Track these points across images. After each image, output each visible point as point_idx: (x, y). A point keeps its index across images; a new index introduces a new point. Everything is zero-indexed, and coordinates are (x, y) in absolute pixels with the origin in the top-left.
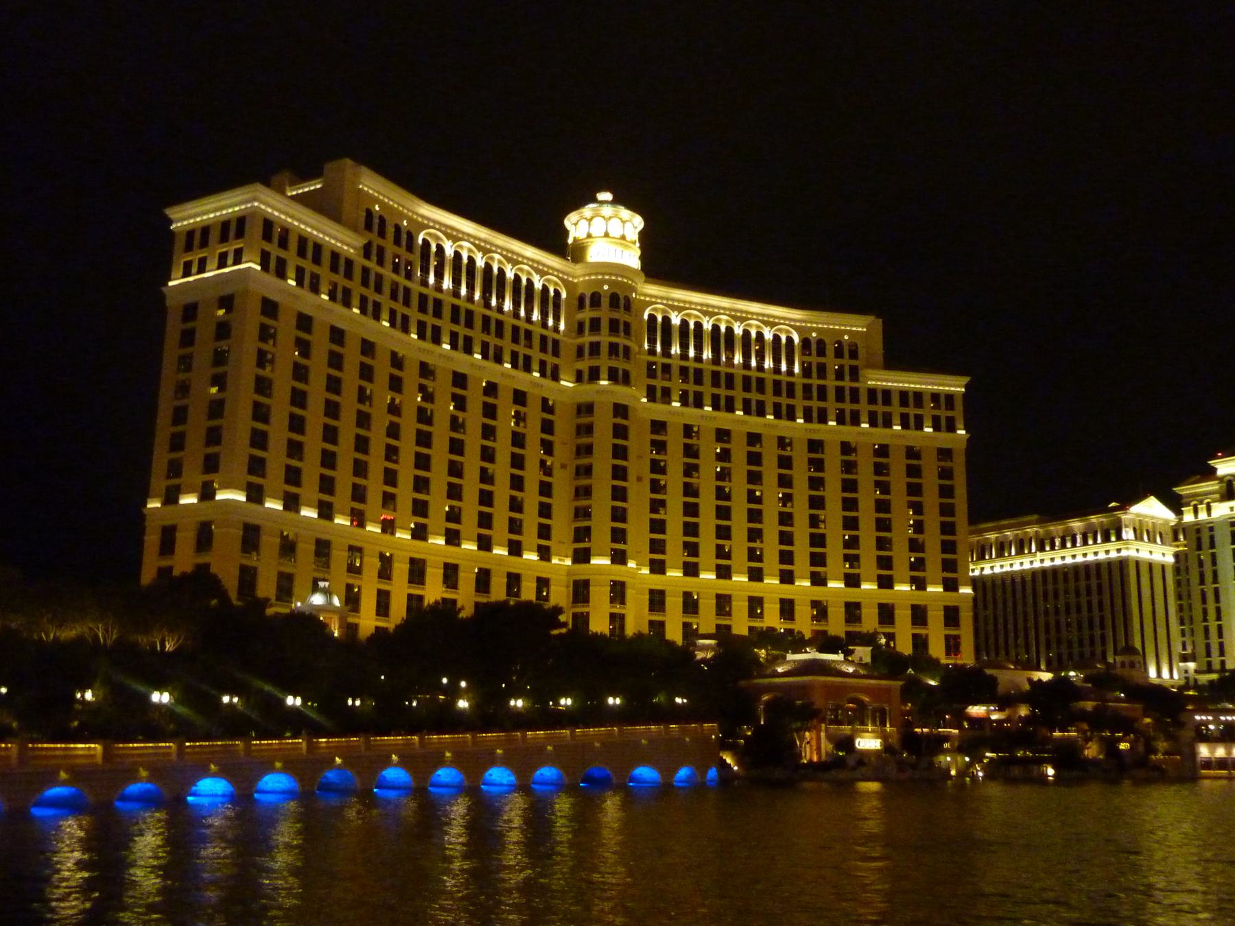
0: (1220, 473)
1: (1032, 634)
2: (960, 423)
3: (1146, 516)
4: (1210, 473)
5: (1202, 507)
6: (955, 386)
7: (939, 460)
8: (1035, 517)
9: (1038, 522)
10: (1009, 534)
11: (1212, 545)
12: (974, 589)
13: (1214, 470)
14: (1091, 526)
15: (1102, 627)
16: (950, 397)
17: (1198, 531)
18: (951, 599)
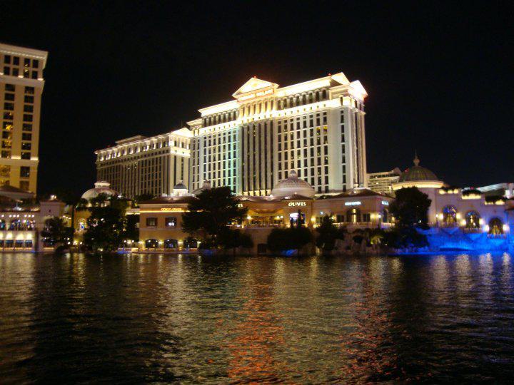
0: (203, 115)
1: (137, 188)
2: (40, 74)
3: (181, 136)
4: (198, 116)
5: (196, 131)
6: (42, 56)
7: (6, 90)
8: (139, 136)
9: (142, 139)
10: (131, 144)
11: (199, 148)
12: (39, 159)
13: (200, 114)
14: (159, 140)
15: (160, 185)
16: (36, 63)
17: (194, 142)
18: (26, 163)
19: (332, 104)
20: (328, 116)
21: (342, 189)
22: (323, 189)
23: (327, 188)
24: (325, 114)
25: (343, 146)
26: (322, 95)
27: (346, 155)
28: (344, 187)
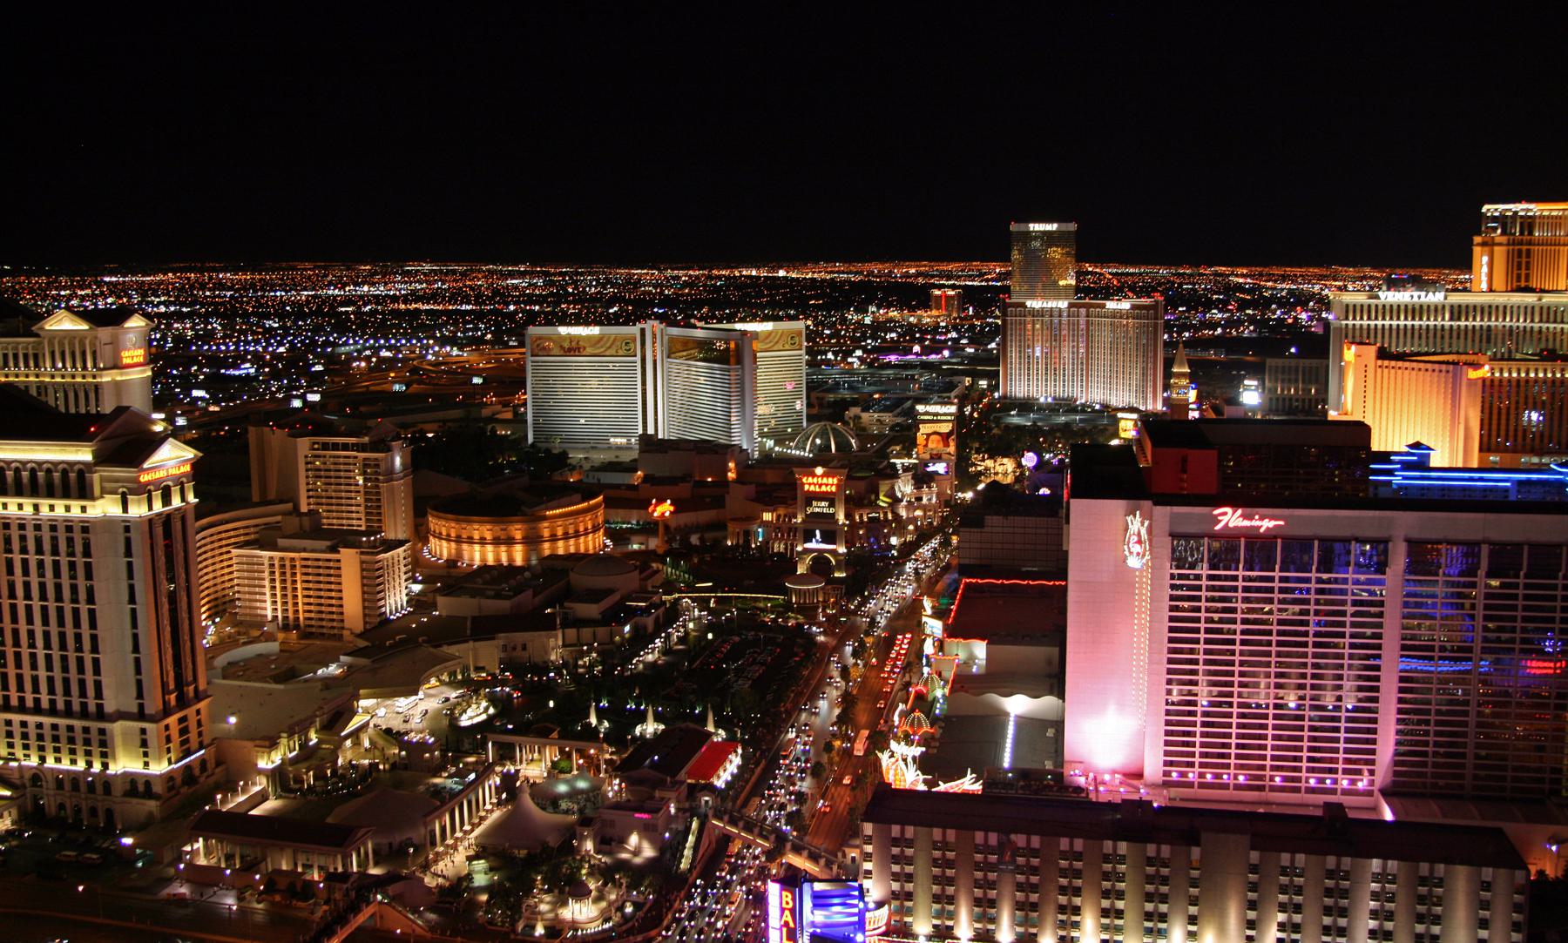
19: (105, 508)
20: (91, 536)
21: (135, 710)
22: (92, 708)
23: (100, 707)
24: (85, 530)
25: (134, 611)
26: (75, 484)
27: (141, 630)
28: (141, 706)
